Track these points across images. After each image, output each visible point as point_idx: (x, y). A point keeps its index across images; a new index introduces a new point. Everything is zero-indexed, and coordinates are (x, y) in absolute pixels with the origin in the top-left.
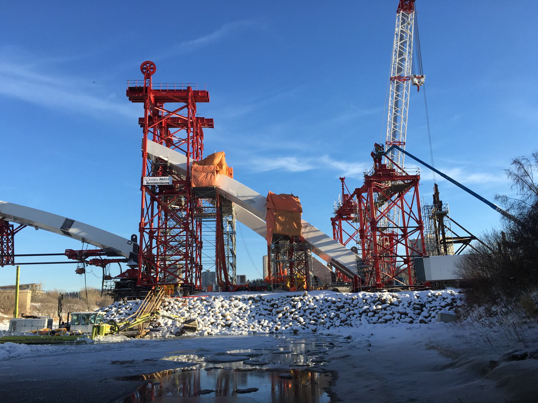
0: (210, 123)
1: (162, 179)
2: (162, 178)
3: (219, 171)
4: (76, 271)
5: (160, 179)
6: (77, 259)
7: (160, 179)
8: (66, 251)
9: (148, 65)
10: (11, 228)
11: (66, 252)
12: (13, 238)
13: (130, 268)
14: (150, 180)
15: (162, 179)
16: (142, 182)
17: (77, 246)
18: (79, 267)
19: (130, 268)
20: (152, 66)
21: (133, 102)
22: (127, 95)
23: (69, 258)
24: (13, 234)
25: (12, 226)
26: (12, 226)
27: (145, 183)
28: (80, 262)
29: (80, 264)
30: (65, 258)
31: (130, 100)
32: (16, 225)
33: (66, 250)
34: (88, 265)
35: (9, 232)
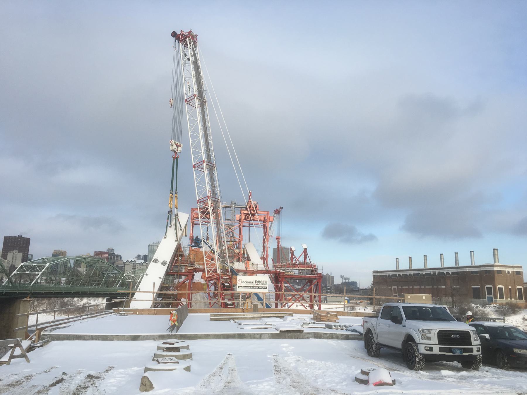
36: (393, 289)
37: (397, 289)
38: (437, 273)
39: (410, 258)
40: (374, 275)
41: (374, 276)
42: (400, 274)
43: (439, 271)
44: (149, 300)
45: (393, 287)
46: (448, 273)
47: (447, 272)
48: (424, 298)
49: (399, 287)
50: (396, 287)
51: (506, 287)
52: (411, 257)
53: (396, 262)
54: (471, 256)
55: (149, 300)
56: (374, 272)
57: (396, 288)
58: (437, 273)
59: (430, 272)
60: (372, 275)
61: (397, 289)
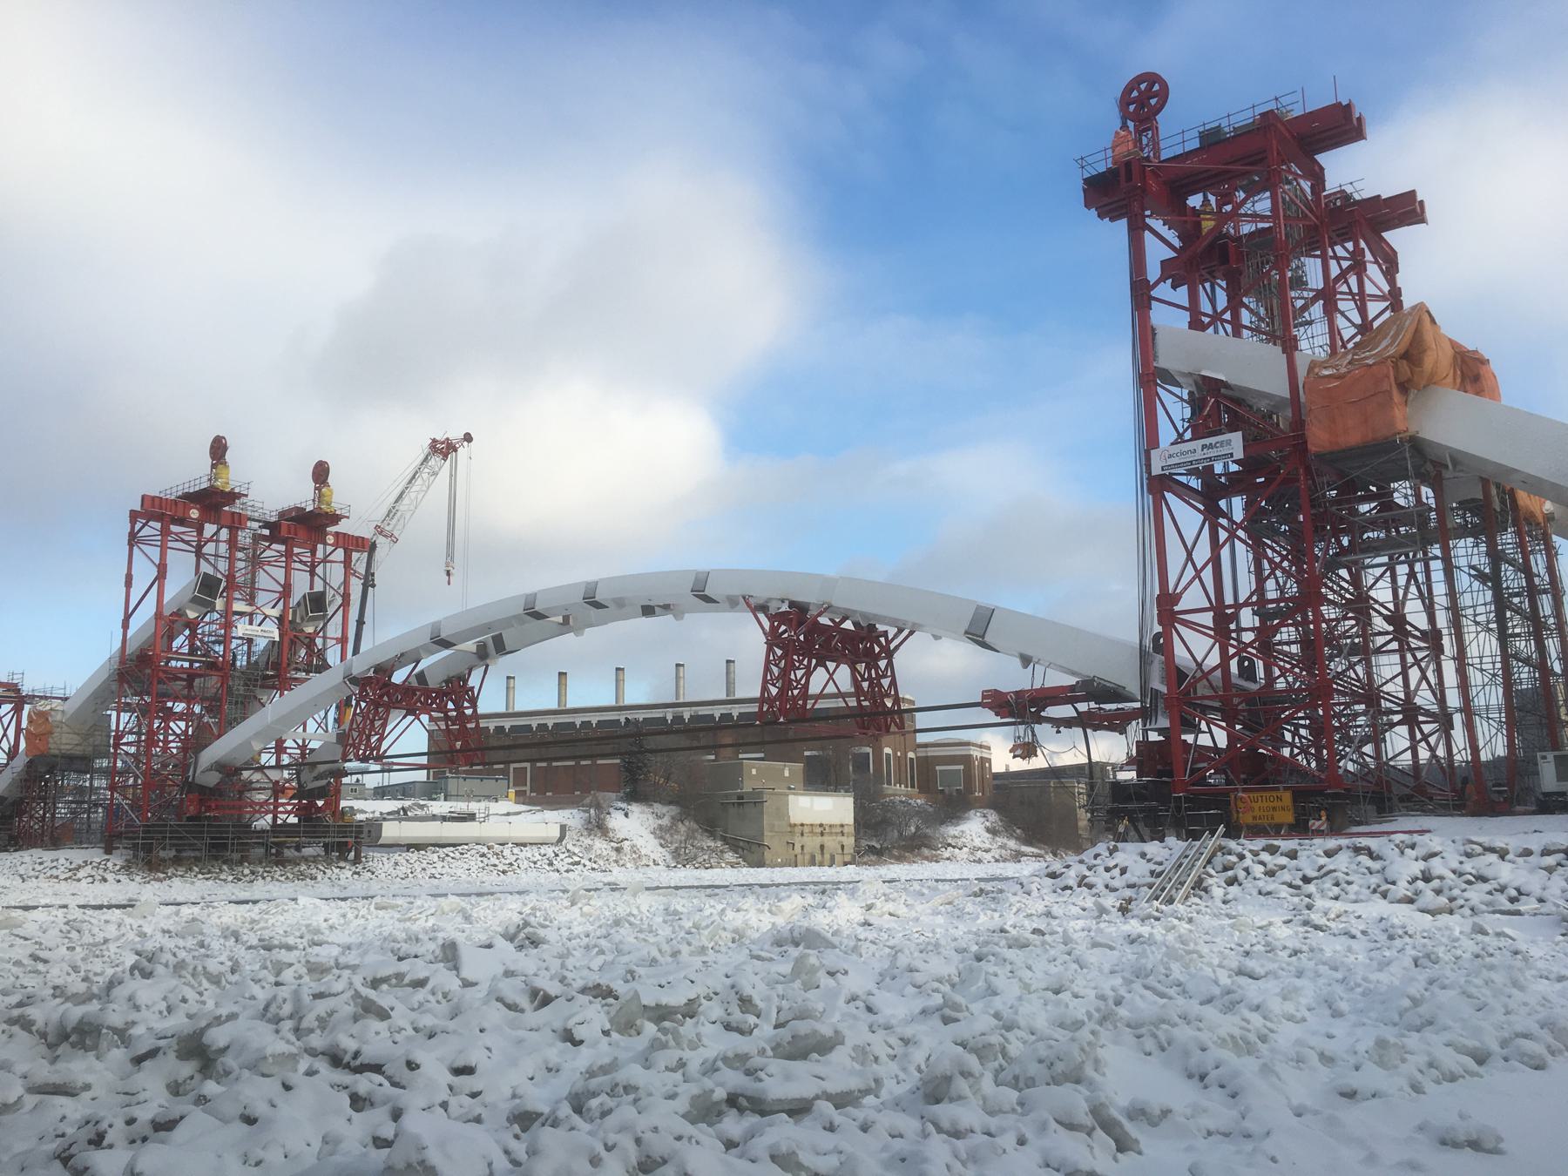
0: (1407, 209)
1: (1211, 446)
2: (1207, 441)
3: (1409, 381)
4: (1011, 751)
5: (1204, 447)
6: (1011, 715)
7: (1204, 447)
8: (984, 696)
9: (1143, 86)
10: (882, 640)
11: (984, 697)
12: (890, 664)
13: (1162, 738)
14: (1170, 456)
15: (1211, 446)
16: (1148, 466)
17: (1014, 679)
18: (1019, 737)
19: (1162, 738)
20: (1156, 87)
21: (1112, 219)
22: (1088, 205)
23: (997, 714)
24: (889, 654)
25: (885, 634)
26: (885, 634)
27: (1156, 470)
28: (1020, 723)
29: (1022, 728)
30: (989, 716)
31: (1101, 216)
32: (892, 632)
33: (983, 692)
34: (1062, 729)
35: (877, 649)
38: (687, 716)
39: (563, 677)
42: (545, 725)
43: (695, 711)
45: (513, 766)
48: (787, 774)
50: (527, 765)
51: (895, 753)
53: (508, 688)
54: (677, 677)
58: (687, 716)
59: (661, 715)
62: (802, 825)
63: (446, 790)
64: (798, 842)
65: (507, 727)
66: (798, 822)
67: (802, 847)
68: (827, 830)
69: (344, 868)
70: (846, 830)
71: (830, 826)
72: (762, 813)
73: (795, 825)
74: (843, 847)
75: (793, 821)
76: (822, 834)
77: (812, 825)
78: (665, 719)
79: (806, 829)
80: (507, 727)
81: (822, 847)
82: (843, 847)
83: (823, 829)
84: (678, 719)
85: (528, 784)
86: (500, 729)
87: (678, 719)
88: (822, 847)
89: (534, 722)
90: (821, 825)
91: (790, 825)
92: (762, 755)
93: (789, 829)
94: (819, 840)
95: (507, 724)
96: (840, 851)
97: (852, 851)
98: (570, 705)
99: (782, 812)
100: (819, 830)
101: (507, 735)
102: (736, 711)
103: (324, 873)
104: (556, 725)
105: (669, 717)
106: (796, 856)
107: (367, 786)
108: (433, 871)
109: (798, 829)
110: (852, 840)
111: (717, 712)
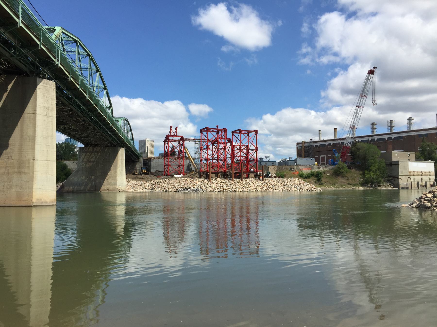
36: (321, 158)
37: (326, 157)
38: (376, 139)
40: (298, 147)
41: (297, 148)
42: (330, 144)
44: (245, 138)
45: (321, 156)
46: (390, 139)
47: (389, 137)
49: (328, 156)
50: (325, 156)
52: (336, 128)
55: (245, 138)
56: (297, 144)
57: (325, 157)
58: (376, 139)
60: (296, 147)
61: (326, 157)
62: (414, 172)
63: (297, 162)
64: (412, 178)
65: (319, 145)
66: (412, 171)
67: (414, 179)
68: (424, 173)
69: (259, 182)
70: (431, 174)
71: (425, 172)
72: (398, 168)
73: (411, 172)
74: (430, 179)
75: (410, 171)
76: (422, 175)
77: (418, 172)
78: (368, 140)
79: (415, 173)
80: (319, 145)
81: (422, 179)
82: (430, 179)
83: (422, 173)
84: (373, 140)
85: (326, 161)
86: (317, 146)
87: (373, 140)
88: (422, 179)
89: (327, 143)
90: (421, 172)
91: (409, 172)
92: (403, 150)
93: (409, 173)
94: (420, 177)
95: (319, 144)
96: (429, 181)
97: (434, 181)
98: (338, 138)
99: (406, 168)
100: (421, 173)
101: (319, 147)
102: (393, 136)
103: (253, 183)
104: (334, 144)
105: (370, 140)
106: (411, 182)
107: (276, 162)
108: (284, 184)
109: (412, 173)
110: (434, 177)
111: (386, 137)
